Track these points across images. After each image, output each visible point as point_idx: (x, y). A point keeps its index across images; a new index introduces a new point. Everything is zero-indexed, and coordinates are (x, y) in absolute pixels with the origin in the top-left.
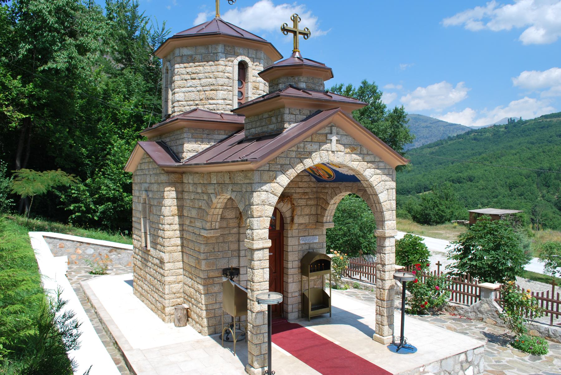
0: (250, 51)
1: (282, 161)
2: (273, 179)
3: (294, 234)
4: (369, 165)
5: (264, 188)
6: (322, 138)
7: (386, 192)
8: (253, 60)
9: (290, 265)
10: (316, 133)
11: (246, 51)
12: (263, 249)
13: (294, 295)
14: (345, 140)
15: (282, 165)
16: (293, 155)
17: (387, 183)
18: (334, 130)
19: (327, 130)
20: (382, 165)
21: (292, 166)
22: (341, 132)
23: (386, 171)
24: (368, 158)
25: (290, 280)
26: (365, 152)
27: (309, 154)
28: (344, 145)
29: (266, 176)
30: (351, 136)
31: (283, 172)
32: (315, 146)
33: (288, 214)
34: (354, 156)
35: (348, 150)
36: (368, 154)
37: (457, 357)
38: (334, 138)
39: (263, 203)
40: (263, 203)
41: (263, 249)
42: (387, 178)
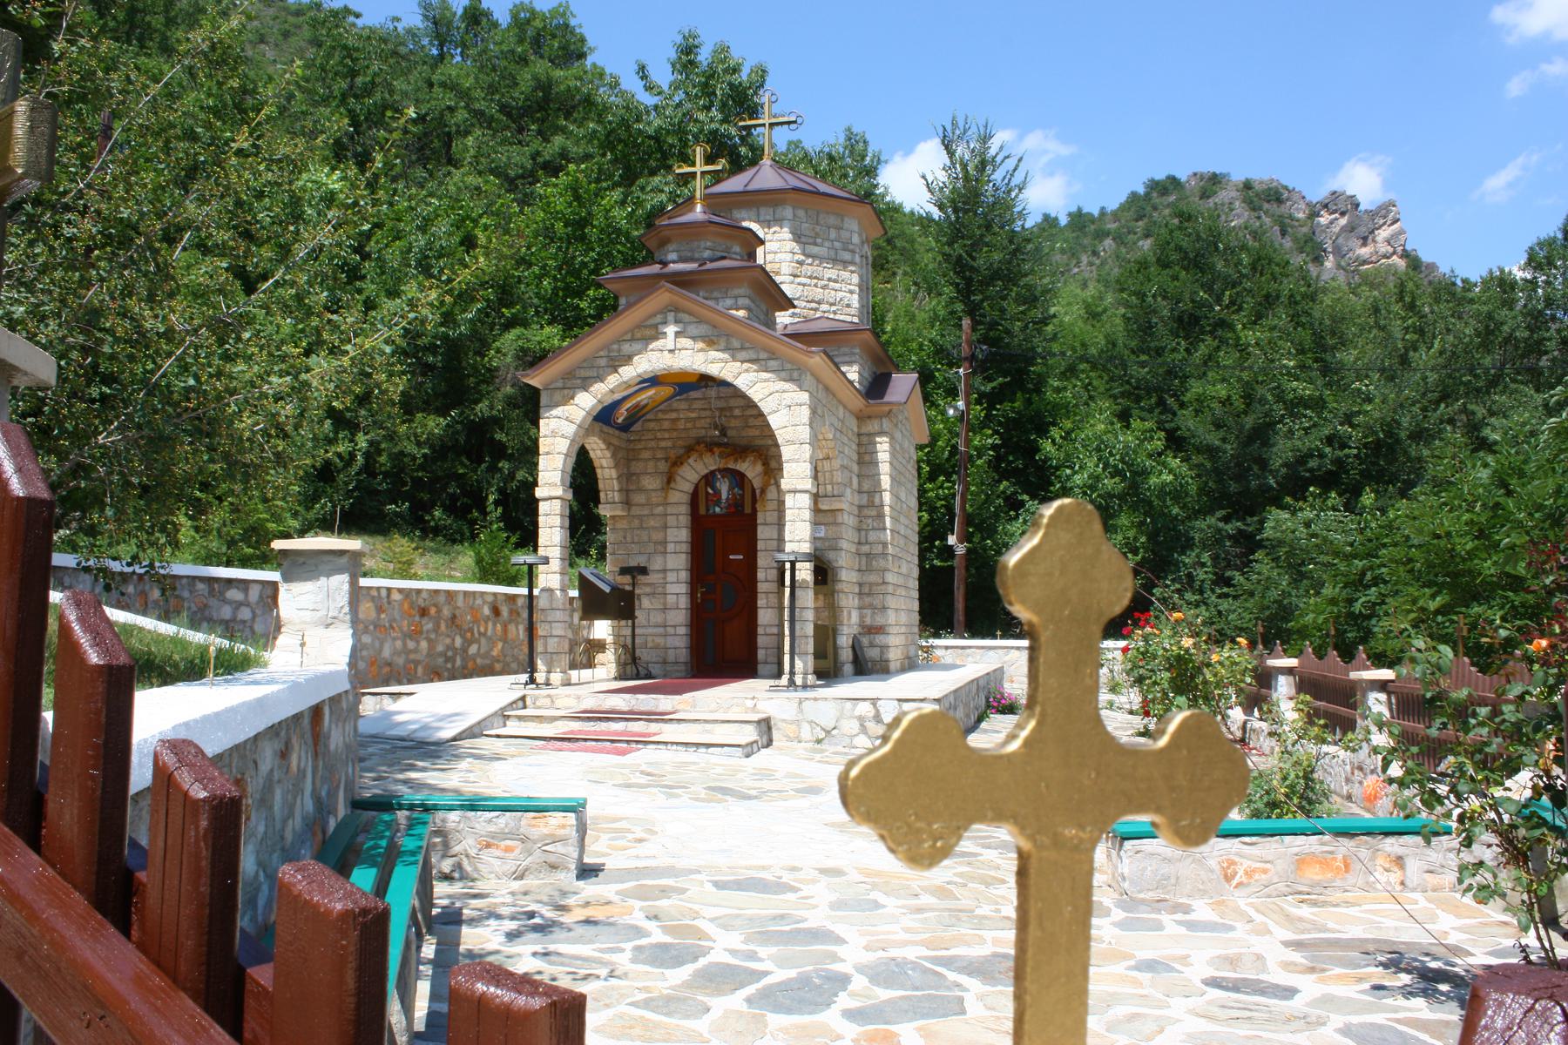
0: (763, 210)
1: (583, 373)
2: (566, 400)
3: (769, 520)
4: (746, 365)
5: (555, 412)
6: (648, 332)
7: (785, 411)
8: (767, 224)
9: (761, 575)
10: (639, 327)
11: (753, 213)
12: (551, 498)
13: (769, 630)
14: (693, 330)
15: (585, 379)
16: (603, 362)
17: (785, 395)
18: (671, 316)
19: (659, 318)
20: (773, 363)
21: (601, 378)
22: (686, 317)
23: (783, 374)
24: (743, 355)
25: (761, 602)
26: (736, 344)
27: (628, 359)
28: (693, 338)
29: (557, 396)
30: (707, 322)
31: (585, 388)
32: (637, 346)
33: (757, 484)
34: (714, 354)
35: (701, 345)
36: (742, 348)
37: (849, 704)
38: (671, 330)
39: (554, 434)
40: (554, 434)
41: (551, 498)
42: (787, 386)
